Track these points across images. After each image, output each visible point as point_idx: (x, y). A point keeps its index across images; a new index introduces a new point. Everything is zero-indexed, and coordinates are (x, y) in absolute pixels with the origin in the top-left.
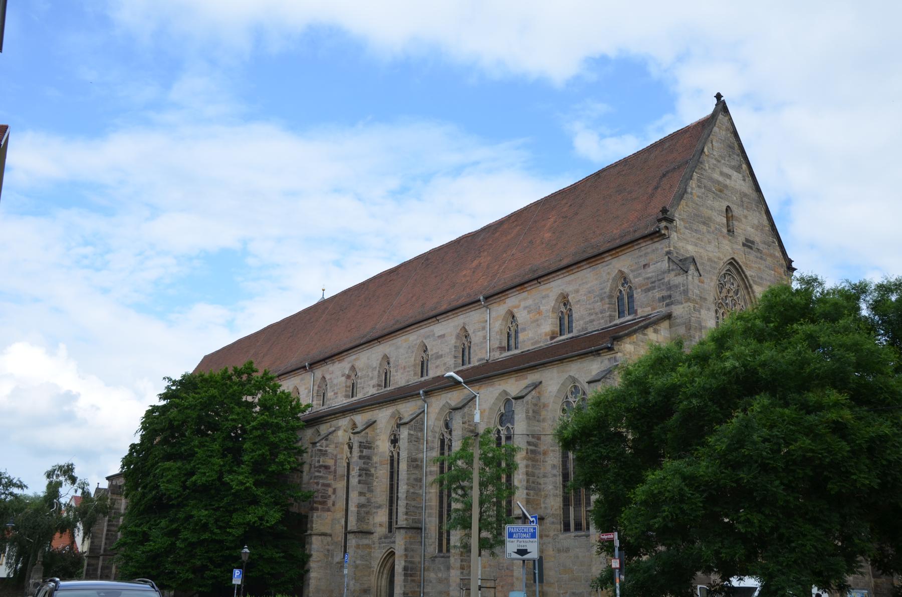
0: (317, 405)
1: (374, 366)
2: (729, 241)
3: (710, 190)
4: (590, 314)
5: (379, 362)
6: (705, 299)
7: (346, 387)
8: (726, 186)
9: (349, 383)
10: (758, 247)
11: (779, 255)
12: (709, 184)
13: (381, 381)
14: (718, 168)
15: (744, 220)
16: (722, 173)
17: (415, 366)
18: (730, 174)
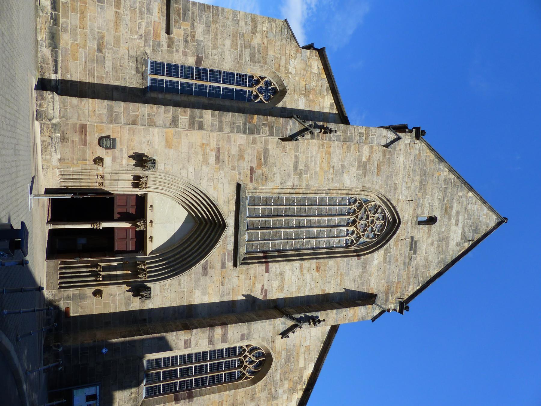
3: (445, 195)
6: (365, 175)
8: (450, 219)
12: (448, 194)
14: (461, 209)
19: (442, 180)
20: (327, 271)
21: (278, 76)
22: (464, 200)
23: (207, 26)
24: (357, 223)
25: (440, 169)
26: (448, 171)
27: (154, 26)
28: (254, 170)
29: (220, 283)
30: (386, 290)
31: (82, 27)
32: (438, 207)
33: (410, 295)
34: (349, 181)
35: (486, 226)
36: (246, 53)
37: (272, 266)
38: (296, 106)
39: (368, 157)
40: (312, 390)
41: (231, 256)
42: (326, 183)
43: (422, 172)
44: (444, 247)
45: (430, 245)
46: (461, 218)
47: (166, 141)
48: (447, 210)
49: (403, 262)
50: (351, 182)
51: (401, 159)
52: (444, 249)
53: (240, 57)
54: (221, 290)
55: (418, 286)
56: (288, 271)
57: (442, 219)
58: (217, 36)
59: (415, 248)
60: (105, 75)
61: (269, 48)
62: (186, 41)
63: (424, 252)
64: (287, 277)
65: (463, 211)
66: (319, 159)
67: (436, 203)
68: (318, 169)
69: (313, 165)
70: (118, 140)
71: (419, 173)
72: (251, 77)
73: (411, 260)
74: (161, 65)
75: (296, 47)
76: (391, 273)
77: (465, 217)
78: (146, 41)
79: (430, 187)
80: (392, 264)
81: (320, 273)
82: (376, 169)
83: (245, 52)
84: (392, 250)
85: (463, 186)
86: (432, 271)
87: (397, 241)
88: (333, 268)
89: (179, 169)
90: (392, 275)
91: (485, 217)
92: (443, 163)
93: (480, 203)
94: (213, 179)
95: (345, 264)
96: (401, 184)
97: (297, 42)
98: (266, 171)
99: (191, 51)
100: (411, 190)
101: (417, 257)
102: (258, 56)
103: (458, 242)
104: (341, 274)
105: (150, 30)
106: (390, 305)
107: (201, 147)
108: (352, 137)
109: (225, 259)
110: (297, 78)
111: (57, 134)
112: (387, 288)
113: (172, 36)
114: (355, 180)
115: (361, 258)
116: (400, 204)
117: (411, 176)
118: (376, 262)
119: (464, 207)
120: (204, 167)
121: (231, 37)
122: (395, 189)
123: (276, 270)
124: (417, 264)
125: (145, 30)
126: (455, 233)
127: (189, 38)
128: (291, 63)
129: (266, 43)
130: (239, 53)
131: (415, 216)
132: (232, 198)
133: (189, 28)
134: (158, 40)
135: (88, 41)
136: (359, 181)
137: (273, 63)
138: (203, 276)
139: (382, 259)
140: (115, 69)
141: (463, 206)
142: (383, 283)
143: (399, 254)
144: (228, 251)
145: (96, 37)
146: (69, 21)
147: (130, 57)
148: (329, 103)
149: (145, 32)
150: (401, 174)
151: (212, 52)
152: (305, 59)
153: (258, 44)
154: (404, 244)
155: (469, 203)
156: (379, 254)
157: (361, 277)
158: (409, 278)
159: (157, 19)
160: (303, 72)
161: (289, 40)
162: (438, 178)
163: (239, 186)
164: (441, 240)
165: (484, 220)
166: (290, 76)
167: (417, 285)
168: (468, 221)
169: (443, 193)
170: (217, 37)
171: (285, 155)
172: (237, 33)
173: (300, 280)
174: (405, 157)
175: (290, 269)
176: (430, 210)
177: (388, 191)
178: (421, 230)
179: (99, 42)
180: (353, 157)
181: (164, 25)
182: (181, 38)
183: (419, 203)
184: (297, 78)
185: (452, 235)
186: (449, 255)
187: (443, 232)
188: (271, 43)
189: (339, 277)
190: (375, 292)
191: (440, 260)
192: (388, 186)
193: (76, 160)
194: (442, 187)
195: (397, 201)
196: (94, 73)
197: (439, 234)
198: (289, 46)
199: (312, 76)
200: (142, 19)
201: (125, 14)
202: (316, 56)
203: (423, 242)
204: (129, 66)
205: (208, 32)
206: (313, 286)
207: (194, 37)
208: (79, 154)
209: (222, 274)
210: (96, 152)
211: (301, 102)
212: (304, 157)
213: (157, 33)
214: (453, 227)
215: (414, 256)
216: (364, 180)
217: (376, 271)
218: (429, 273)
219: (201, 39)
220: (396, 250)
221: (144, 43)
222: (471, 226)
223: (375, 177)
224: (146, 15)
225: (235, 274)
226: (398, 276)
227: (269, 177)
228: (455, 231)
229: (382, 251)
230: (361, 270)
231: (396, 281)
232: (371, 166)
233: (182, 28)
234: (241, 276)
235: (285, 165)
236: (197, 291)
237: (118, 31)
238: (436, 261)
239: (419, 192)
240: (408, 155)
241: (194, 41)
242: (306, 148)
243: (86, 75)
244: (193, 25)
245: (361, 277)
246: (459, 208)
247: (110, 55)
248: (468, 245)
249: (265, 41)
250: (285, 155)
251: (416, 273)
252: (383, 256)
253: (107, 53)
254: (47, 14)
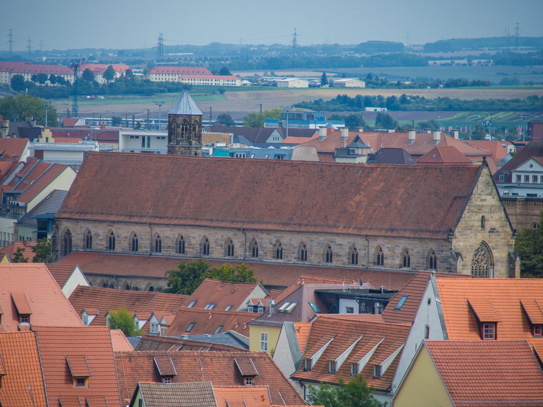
0: (249, 255)
1: (295, 245)
2: (482, 233)
3: (474, 212)
4: (418, 263)
5: (298, 245)
7: (273, 251)
8: (483, 206)
9: (275, 249)
13: (300, 256)
15: (491, 219)
16: (481, 200)
17: (323, 255)
25: (464, 217)
48: (480, 208)
174: (460, 241)
190: (507, 253)
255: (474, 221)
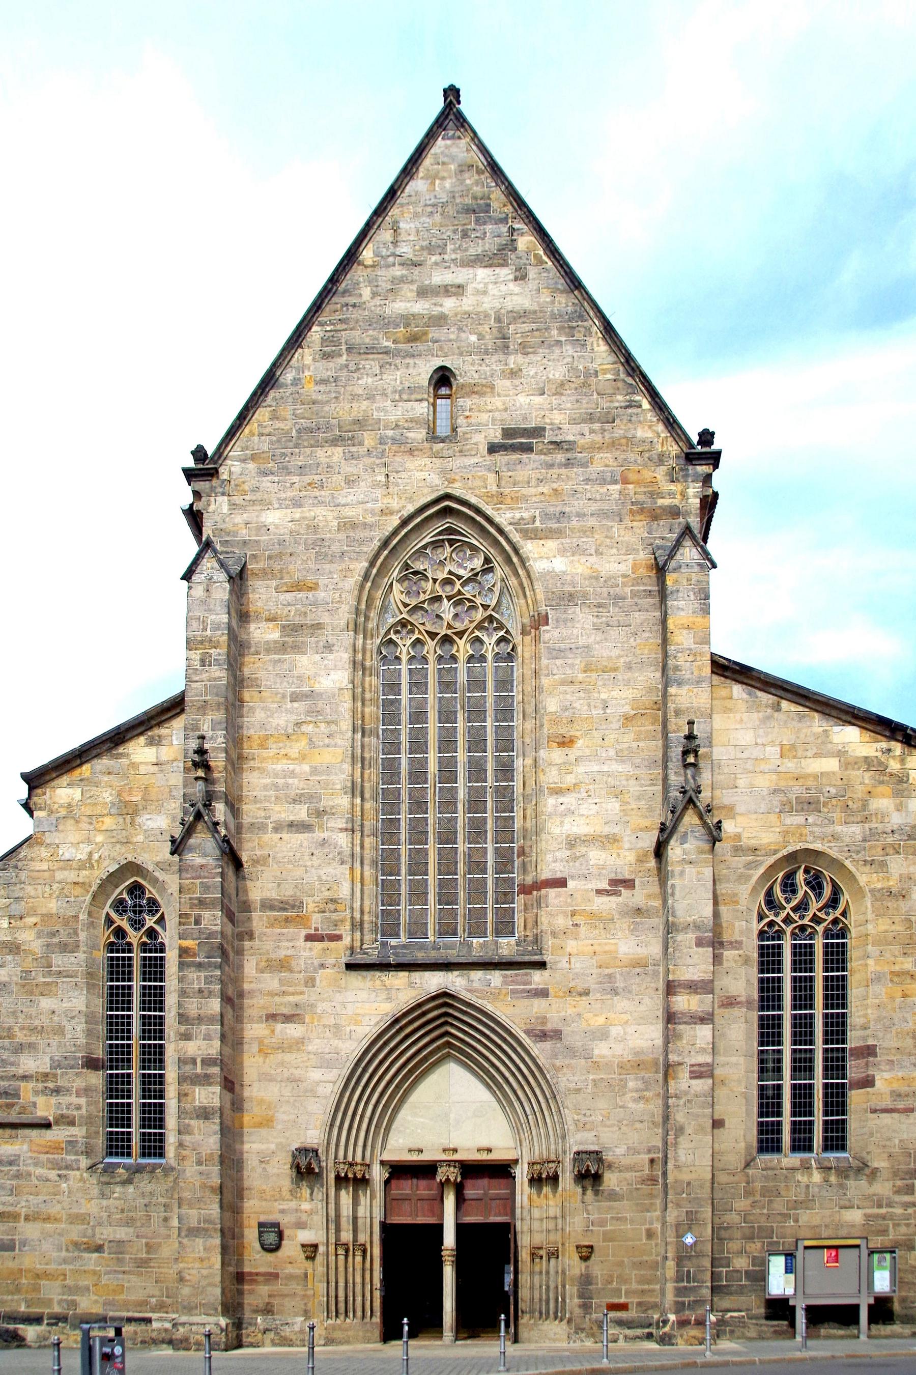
2: (437, 456)
3: (370, 350)
6: (318, 626)
8: (440, 320)
10: (558, 439)
11: (649, 434)
14: (412, 282)
18: (459, 280)
19: (326, 369)
20: (574, 713)
21: (100, 886)
22: (385, 275)
23: (20, 1048)
24: (449, 632)
25: (296, 382)
26: (300, 350)
27: (40, 1153)
28: (313, 932)
29: (584, 998)
30: (642, 517)
31: (62, 1277)
32: (405, 370)
33: (664, 434)
34: (332, 672)
35: (466, 175)
36: (60, 962)
37: (550, 870)
38: (160, 836)
39: (271, 624)
40: (907, 727)
41: (516, 975)
42: (339, 742)
43: (306, 444)
44: (526, 327)
45: (517, 382)
46: (439, 278)
47: (259, 1127)
49: (563, 471)
50: (335, 668)
51: (272, 517)
52: (534, 326)
53: (72, 977)
54: (598, 996)
55: (640, 406)
56: (567, 827)
57: (441, 348)
58: (36, 1028)
59: (526, 432)
60: (144, 1241)
61: (44, 911)
62: (57, 1091)
63: (538, 400)
64: (579, 827)
65: (416, 270)
66: (279, 767)
67: (394, 378)
68: (306, 768)
69: (296, 780)
70: (263, 1218)
71: (308, 450)
72: (111, 947)
73: (557, 444)
74: (111, 1136)
75: (30, 846)
76: (594, 507)
77: (436, 264)
78: (67, 1167)
79: (348, 406)
80: (567, 509)
81: (578, 734)
82: (301, 595)
83: (59, 966)
84: (526, 515)
85: (343, 285)
86: (599, 361)
87: (499, 499)
88: (568, 696)
89: (317, 1099)
90: (599, 503)
91: (437, 182)
92: (278, 373)
93: (394, 211)
94: (336, 1026)
95: (559, 662)
96: (339, 508)
97: (20, 845)
98: (314, 902)
99: (74, 1081)
100: (355, 472)
101: (552, 424)
102: (63, 937)
103: (511, 277)
104: (585, 672)
105: (48, 1159)
106: (690, 501)
107: (266, 1055)
108: (215, 686)
109: (523, 991)
110: (99, 838)
111: (259, 1321)
112: (638, 517)
113: (51, 1118)
114: (331, 657)
115: (544, 613)
116: (395, 504)
117: (317, 477)
118: (560, 564)
119: (405, 272)
120: (310, 1048)
121: (33, 998)
122: (354, 526)
123: (561, 860)
124: (573, 421)
125: (49, 1169)
126: (485, 293)
127: (51, 1085)
128: (67, 856)
129: (34, 920)
130: (65, 979)
131: (431, 449)
132: (378, 982)
133: (31, 1085)
134: (64, 1145)
135: (86, 1268)
136: (333, 645)
137: (72, 899)
138: (561, 1040)
139: (551, 544)
140: (129, 1222)
141: (402, 276)
142: (622, 533)
143: (540, 489)
144: (507, 984)
145: (76, 1254)
146: (56, 1298)
147: (103, 1195)
148: (147, 749)
149: (53, 1169)
150: (313, 514)
151: (70, 1036)
152: (54, 822)
153: (39, 935)
154: (510, 474)
155: (394, 255)
156: (536, 556)
157: (599, 606)
158: (613, 444)
159: (25, 1147)
160: (84, 826)
161: (20, 864)
162: (323, 381)
163: (350, 967)
164: (503, 344)
165: (448, 184)
166: (96, 856)
167: (635, 410)
168: (450, 247)
169: (364, 357)
170: (39, 1028)
171: (274, 858)
172: (24, 986)
173: (592, 793)
174: (266, 505)
175: (562, 822)
176: (413, 397)
177: (357, 550)
178: (472, 420)
179: (85, 1249)
180: (270, 668)
181: (34, 1133)
182: (53, 1100)
183: (393, 439)
184: (99, 838)
185: (489, 304)
186: (553, 302)
187: (481, 337)
188: (32, 908)
189: (594, 675)
191: (567, 335)
192: (347, 552)
193: (306, 1290)
194: (347, 366)
195: (386, 515)
196: (141, 1259)
197: (486, 352)
198: (33, 863)
199: (89, 801)
200: (30, 1175)
201: (27, 1204)
202: (44, 794)
203: (506, 410)
204: (119, 1199)
205: (32, 1046)
206: (612, 753)
207: (46, 1075)
208: (297, 1288)
209: (561, 994)
210: (289, 1257)
211: (151, 824)
212: (277, 808)
213: (50, 1146)
214: (467, 303)
215: (549, 436)
216: (330, 628)
217: (583, 559)
218: (605, 372)
219: (48, 1060)
220: (525, 499)
221: (73, 1170)
222: (465, 235)
223: (321, 595)
224: (21, 1168)
225: (564, 964)
226: (603, 482)
227: (327, 893)
228: (478, 292)
229: (529, 548)
230: (578, 609)
231: (618, 487)
232: (292, 613)
233: (33, 1099)
234: (569, 949)
235: (298, 855)
236: (596, 1052)
237: (59, 1216)
238: (569, 350)
239: (361, 444)
240: (258, 496)
241: (55, 1076)
242: (255, 803)
243: (147, 1272)
244: (25, 1078)
245: (599, 606)
246: (408, 290)
247: (105, 1232)
248: (522, 234)
249: (31, 920)
250: (274, 858)
251: (599, 421)
252: (542, 542)
253: (102, 1237)
254: (49, 1332)
255: (370, 398)
